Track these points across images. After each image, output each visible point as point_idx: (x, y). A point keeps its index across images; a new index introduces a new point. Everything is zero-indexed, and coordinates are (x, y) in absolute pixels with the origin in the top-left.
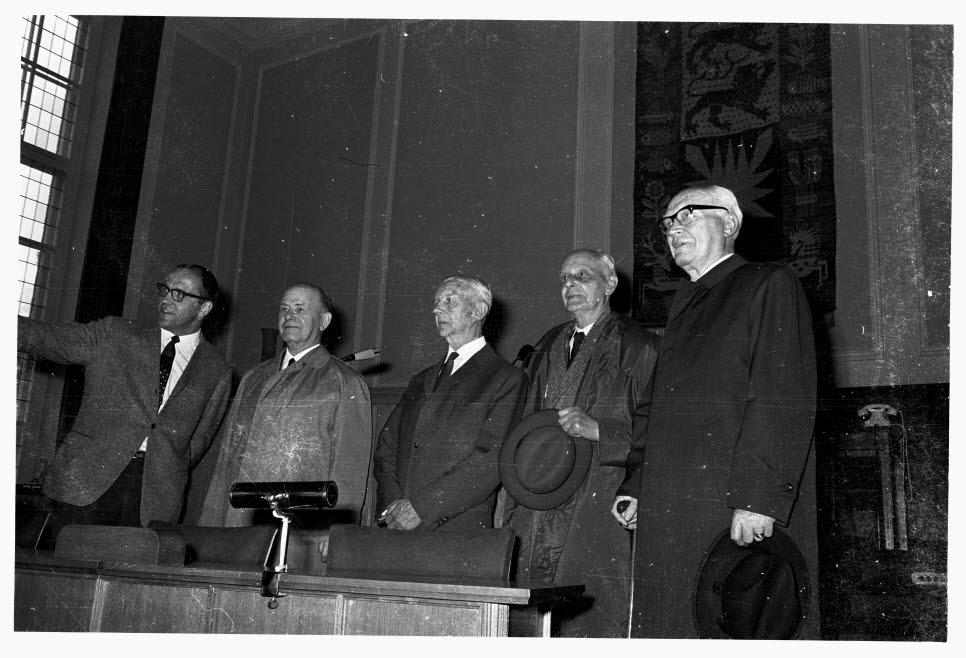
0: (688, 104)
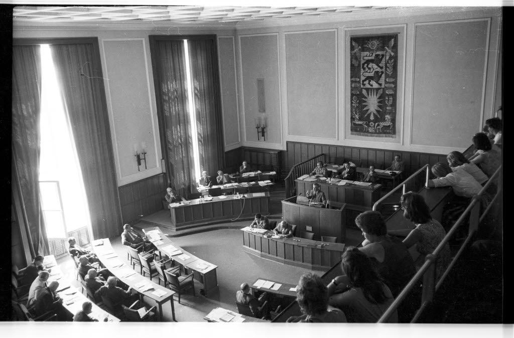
0: (363, 78)
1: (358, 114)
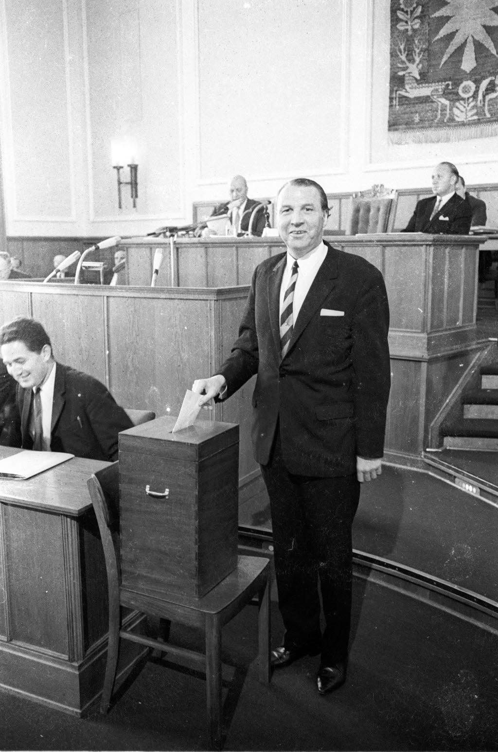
1: (417, 59)
